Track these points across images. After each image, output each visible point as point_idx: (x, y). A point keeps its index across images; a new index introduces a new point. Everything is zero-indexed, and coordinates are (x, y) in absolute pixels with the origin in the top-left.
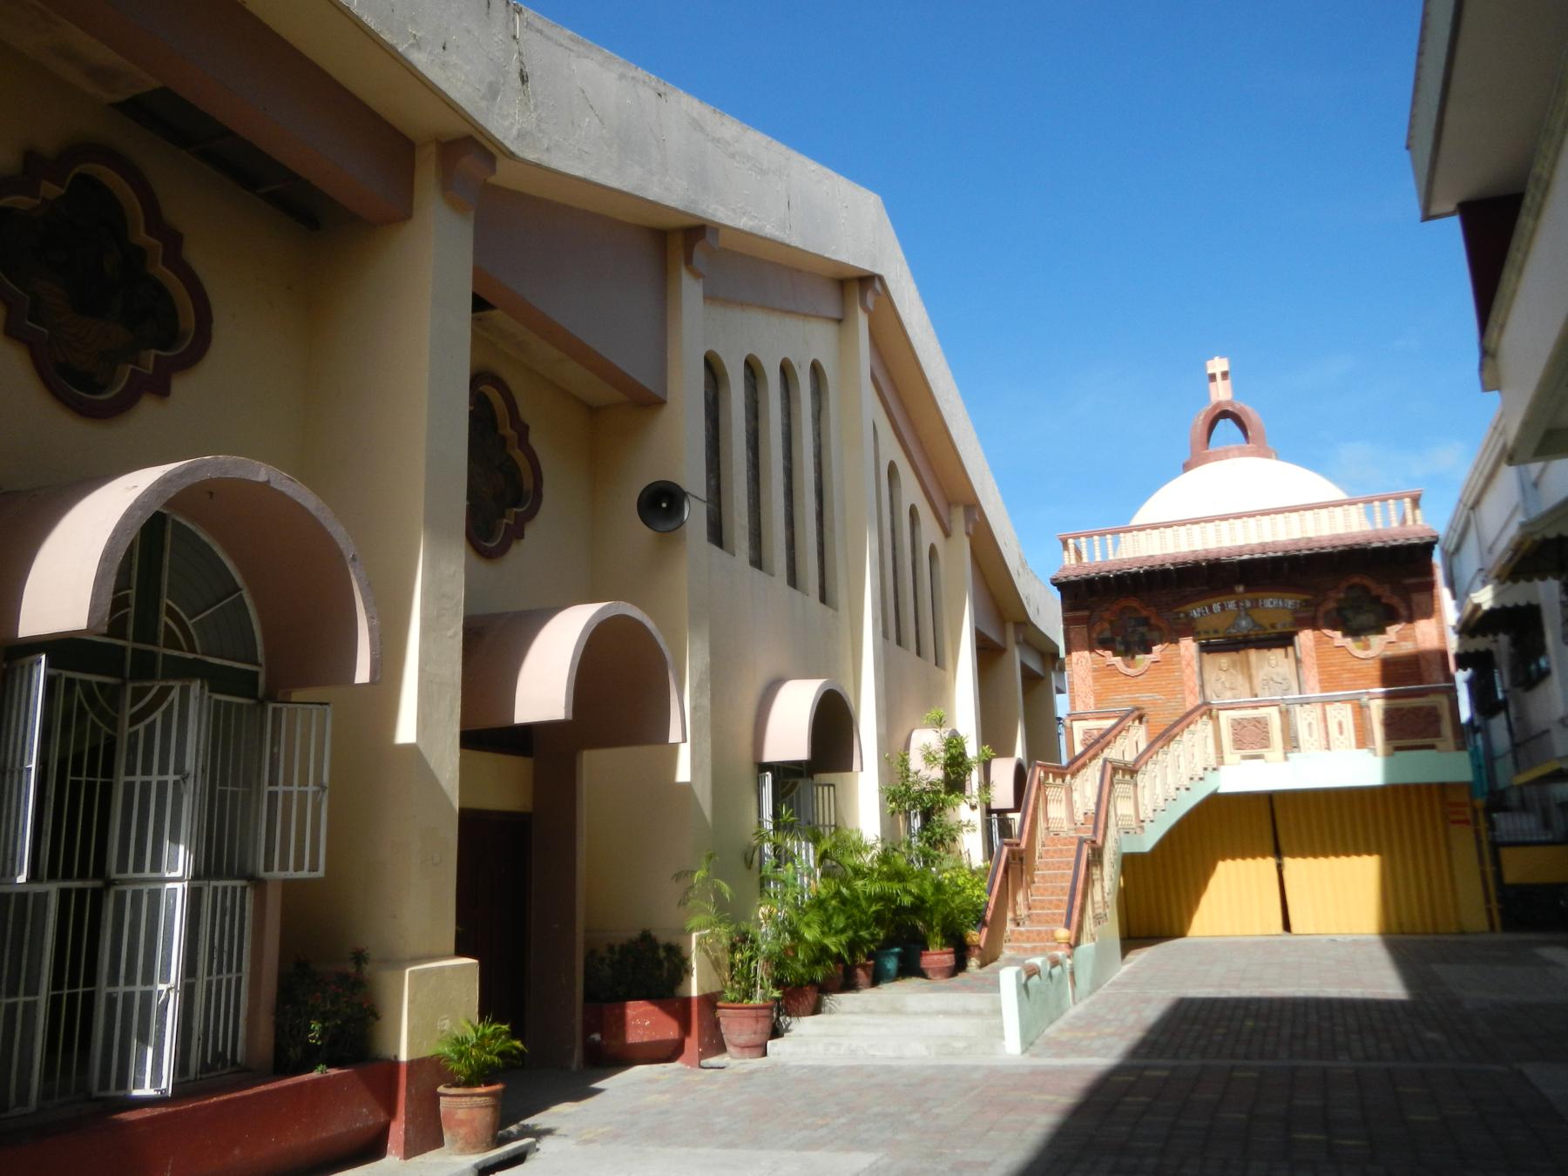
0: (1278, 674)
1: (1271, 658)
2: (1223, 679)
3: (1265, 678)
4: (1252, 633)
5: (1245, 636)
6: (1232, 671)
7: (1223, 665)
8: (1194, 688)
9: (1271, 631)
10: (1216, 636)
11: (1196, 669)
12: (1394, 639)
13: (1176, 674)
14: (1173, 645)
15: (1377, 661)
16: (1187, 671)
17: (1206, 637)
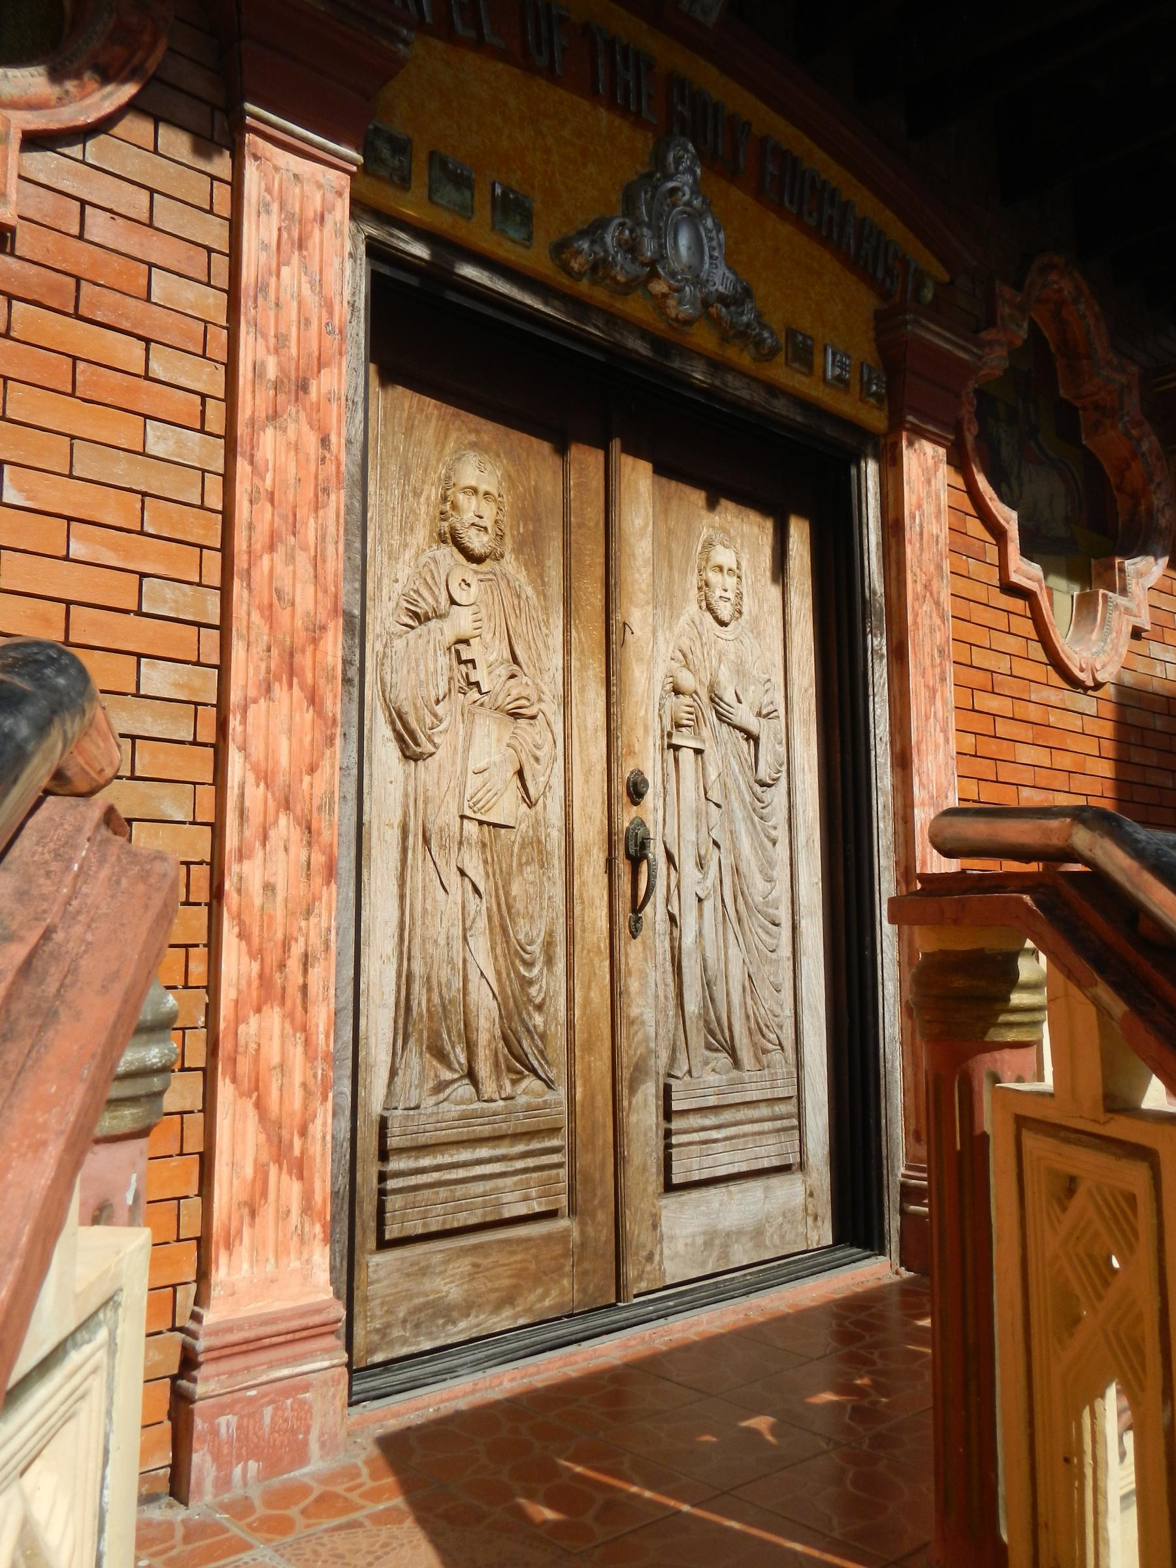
0: (740, 671)
1: (724, 556)
2: (462, 622)
3: (687, 680)
4: (704, 338)
5: (659, 344)
6: (510, 565)
7: (470, 507)
8: (316, 633)
9: (782, 373)
10: (508, 251)
11: (347, 462)
12: (1145, 622)
13: (161, 441)
14: (176, 142)
15: (1108, 710)
16: (269, 443)
17: (442, 220)
